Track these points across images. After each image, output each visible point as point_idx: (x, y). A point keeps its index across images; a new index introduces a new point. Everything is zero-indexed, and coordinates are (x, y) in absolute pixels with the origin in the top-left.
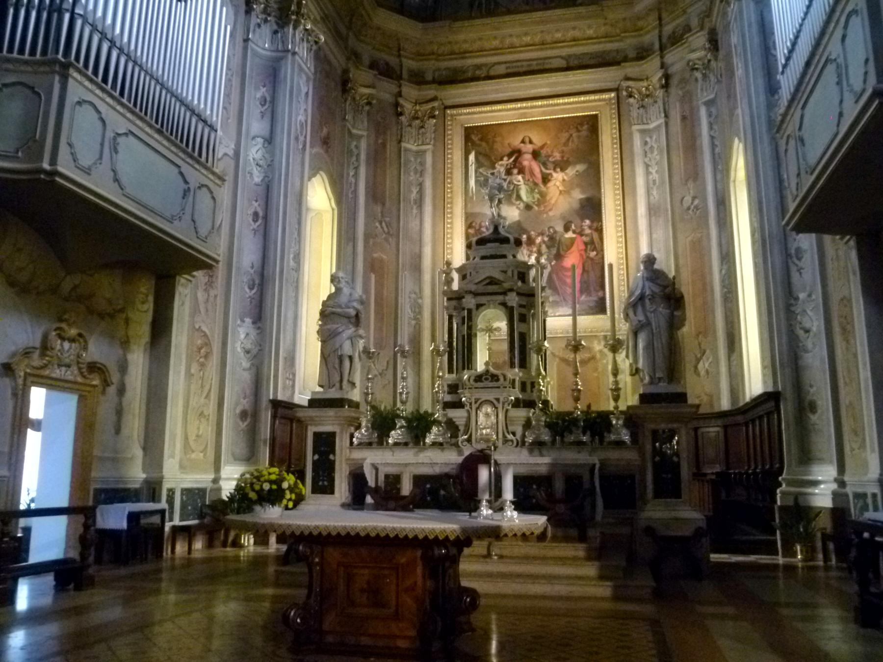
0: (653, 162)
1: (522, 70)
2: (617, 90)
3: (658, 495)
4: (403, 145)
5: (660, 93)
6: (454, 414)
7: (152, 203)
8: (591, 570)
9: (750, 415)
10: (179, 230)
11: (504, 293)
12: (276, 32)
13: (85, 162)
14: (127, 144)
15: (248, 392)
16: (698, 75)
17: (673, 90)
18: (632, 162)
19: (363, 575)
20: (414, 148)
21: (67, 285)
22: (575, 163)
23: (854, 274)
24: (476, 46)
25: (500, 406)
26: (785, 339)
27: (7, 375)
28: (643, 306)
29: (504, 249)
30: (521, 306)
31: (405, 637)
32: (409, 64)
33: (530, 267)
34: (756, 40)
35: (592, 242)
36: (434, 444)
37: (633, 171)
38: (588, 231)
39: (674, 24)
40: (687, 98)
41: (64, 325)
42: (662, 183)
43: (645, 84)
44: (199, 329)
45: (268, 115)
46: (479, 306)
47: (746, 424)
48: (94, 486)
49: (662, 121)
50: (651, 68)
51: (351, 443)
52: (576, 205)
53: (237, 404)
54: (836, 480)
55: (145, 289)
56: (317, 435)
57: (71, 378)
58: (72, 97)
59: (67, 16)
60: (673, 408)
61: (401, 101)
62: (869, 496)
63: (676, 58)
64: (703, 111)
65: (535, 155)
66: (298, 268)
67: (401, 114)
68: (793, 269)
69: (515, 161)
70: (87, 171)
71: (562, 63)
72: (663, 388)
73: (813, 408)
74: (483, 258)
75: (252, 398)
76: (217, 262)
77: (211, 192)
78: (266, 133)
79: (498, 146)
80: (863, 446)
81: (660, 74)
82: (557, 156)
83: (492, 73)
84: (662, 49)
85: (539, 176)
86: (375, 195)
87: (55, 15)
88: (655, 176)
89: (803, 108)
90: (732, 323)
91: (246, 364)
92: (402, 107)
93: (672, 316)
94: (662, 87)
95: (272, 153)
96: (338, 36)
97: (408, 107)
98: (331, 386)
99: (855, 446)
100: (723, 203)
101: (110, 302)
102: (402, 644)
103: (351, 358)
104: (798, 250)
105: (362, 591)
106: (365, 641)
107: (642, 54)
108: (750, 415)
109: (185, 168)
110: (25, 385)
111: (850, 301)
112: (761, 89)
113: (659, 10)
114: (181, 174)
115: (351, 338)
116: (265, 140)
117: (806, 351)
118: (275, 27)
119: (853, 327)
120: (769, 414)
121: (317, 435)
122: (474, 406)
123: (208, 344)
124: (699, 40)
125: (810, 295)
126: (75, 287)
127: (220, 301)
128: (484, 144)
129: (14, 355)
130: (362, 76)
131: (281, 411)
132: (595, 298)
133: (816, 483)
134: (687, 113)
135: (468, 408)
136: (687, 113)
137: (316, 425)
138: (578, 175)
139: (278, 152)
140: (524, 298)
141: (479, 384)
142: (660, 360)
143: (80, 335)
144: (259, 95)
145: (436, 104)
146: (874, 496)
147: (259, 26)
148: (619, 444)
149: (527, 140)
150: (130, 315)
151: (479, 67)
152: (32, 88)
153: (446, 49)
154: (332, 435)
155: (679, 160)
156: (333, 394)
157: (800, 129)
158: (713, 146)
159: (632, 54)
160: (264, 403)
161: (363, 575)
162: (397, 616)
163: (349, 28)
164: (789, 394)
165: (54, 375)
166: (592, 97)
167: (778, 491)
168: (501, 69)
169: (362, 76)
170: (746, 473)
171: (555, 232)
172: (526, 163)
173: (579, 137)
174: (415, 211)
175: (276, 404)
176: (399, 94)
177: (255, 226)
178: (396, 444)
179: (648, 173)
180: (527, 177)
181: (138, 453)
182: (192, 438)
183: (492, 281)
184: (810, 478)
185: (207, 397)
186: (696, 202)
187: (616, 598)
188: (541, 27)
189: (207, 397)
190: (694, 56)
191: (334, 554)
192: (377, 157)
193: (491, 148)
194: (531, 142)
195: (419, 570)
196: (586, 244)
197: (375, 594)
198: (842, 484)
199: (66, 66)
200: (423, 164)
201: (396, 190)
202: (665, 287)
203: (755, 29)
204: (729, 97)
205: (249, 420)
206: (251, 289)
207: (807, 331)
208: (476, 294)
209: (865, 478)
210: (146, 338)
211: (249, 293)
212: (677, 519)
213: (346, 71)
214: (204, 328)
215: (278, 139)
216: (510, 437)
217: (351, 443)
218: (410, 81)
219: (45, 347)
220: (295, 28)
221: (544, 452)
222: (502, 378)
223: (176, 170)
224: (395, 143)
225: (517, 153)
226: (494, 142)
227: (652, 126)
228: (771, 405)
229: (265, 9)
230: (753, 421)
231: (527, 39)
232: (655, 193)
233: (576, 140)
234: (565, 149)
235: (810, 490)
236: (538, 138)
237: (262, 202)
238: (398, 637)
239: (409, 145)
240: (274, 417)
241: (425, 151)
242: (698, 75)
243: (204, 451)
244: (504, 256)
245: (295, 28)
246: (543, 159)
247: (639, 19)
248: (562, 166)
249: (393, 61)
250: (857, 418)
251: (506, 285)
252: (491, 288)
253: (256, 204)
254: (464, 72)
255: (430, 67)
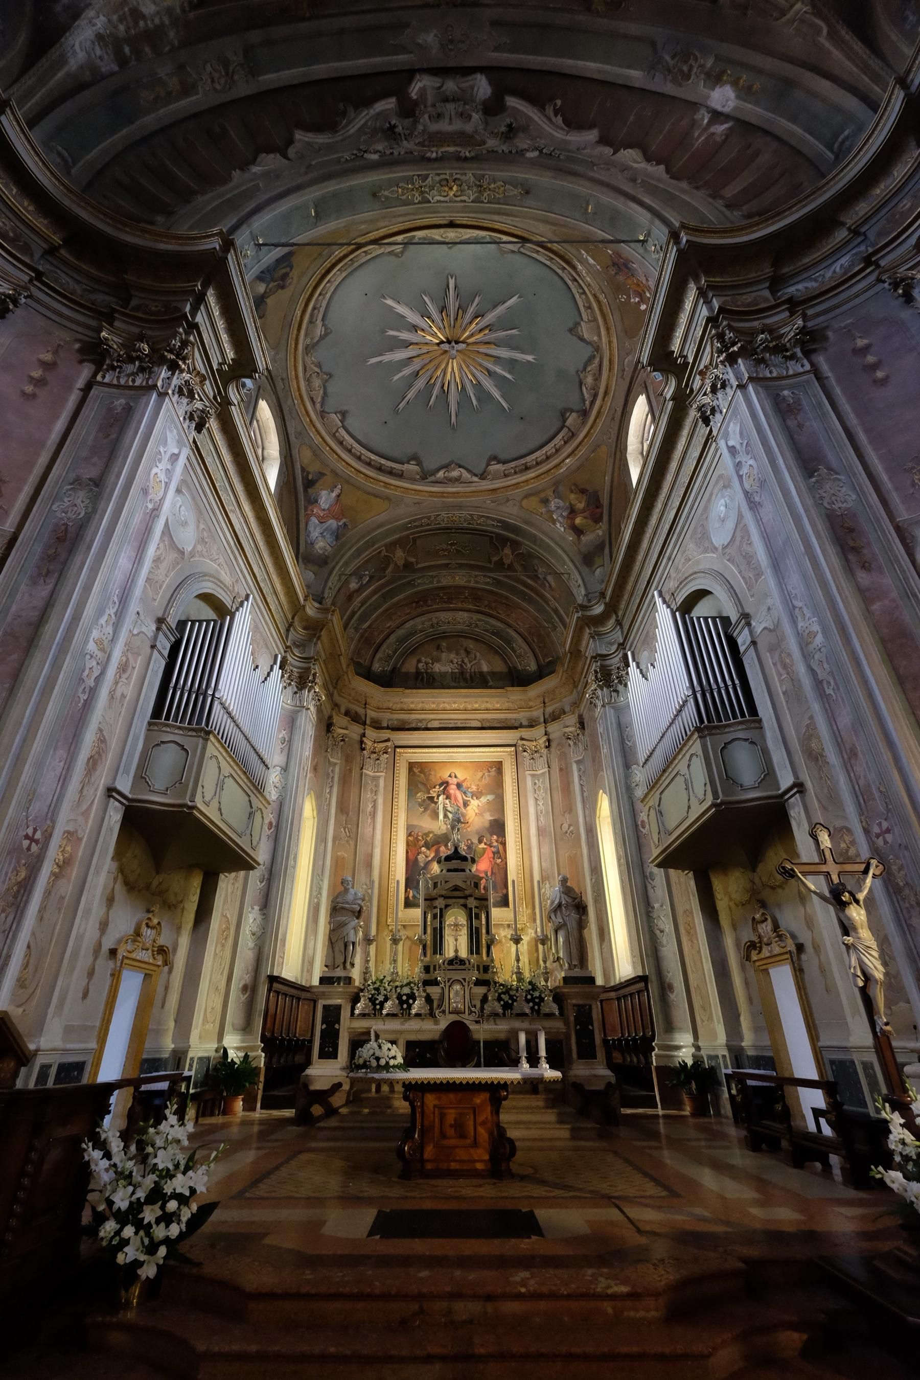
0: (540, 798)
1: (450, 726)
2: (515, 745)
3: (580, 1057)
4: (364, 771)
5: (544, 751)
6: (431, 990)
7: (234, 825)
8: (550, 1116)
9: (622, 992)
10: (244, 843)
11: (466, 897)
12: (296, 693)
13: (207, 799)
14: (229, 782)
15: (250, 968)
16: (571, 743)
17: (553, 749)
18: (526, 797)
19: (451, 1115)
20: (371, 774)
21: (155, 883)
22: (487, 794)
23: (694, 896)
24: (420, 706)
25: (466, 984)
26: (647, 936)
27: (110, 959)
28: (561, 912)
29: (461, 865)
30: (476, 907)
31: (482, 1161)
32: (372, 714)
33: (481, 878)
34: (616, 734)
35: (498, 852)
36: (418, 1015)
37: (527, 802)
38: (495, 844)
39: (554, 707)
40: (563, 756)
41: (150, 915)
42: (547, 812)
43: (534, 744)
44: (226, 916)
45: (286, 751)
46: (447, 906)
47: (618, 999)
48: (144, 1057)
49: (547, 770)
50: (539, 731)
51: (352, 1014)
52: (487, 824)
53: (240, 980)
54: (693, 1045)
55: (196, 882)
56: (325, 1007)
57: (146, 960)
58: (208, 754)
59: (209, 699)
60: (586, 988)
61: (364, 739)
62: (720, 1057)
63: (555, 729)
64: (575, 767)
65: (459, 786)
66: (294, 867)
67: (364, 749)
68: (649, 887)
69: (444, 789)
70: (207, 804)
71: (479, 725)
72: (577, 972)
73: (671, 988)
74: (449, 871)
75: (253, 974)
76: (259, 864)
77: (262, 813)
78: (283, 764)
79: (432, 777)
80: (710, 1018)
81: (545, 738)
82: (474, 788)
83: (429, 726)
84: (545, 722)
85: (461, 801)
86: (342, 808)
87: (201, 698)
88: (541, 807)
89: (661, 793)
90: (602, 919)
91: (251, 944)
92: (365, 744)
93: (580, 919)
94: (546, 747)
95: (286, 779)
96: (330, 695)
97: (369, 743)
98: (335, 967)
99: (704, 1018)
100: (592, 832)
101: (176, 894)
102: (479, 1166)
103: (354, 943)
104: (651, 873)
105: (451, 1126)
106: (454, 1166)
107: (532, 725)
108: (622, 992)
109: (253, 798)
110: (121, 966)
111: (691, 913)
112: (620, 763)
113: (544, 697)
114: (250, 801)
115: (355, 928)
116: (282, 768)
117: (663, 946)
118: (296, 690)
119: (696, 932)
120: (639, 992)
121: (325, 1007)
122: (448, 984)
123: (228, 928)
124: (571, 720)
125: (662, 906)
126: (160, 884)
127: (239, 893)
128: (422, 775)
129: (119, 941)
130: (340, 720)
131: (276, 986)
132: (501, 895)
133: (678, 1048)
134: (563, 767)
135: (442, 985)
136: (563, 767)
137: (326, 999)
138: (489, 802)
139: (290, 777)
140: (478, 902)
141: (451, 967)
142: (574, 951)
143: (159, 923)
144: (280, 736)
145: (389, 744)
146: (724, 1056)
147: (285, 688)
148: (550, 1015)
149: (453, 775)
150: (186, 906)
151: (421, 721)
152: (182, 747)
153: (399, 706)
154: (338, 1008)
155: (558, 797)
156: (339, 973)
157: (659, 805)
158: (582, 791)
159: (525, 723)
160: (263, 978)
161: (451, 1115)
162: (475, 1144)
163: (335, 688)
164: (653, 978)
165: (138, 958)
166: (499, 749)
167: (653, 1054)
168: (436, 724)
169: (340, 720)
170: (619, 1040)
171: (472, 843)
172: (452, 792)
173: (489, 776)
174: (369, 821)
175: (274, 980)
176: (363, 735)
177: (269, 832)
178: (388, 1015)
179: (537, 805)
180: (453, 801)
181: (172, 1024)
182: (209, 1010)
183: (456, 888)
184: (676, 1043)
185: (222, 974)
186: (572, 828)
187: (574, 1138)
188: (466, 700)
189: (222, 974)
190: (567, 730)
191: (430, 1099)
192: (345, 781)
193: (428, 780)
194: (456, 777)
195: (489, 1108)
196: (494, 853)
197: (459, 1128)
198: (698, 1048)
199: (208, 733)
200: (377, 786)
201: (357, 804)
202: (575, 899)
203: (615, 726)
204: (594, 761)
205: (248, 993)
206: (261, 882)
207: (662, 931)
208: (446, 897)
209: (716, 1044)
210: (190, 924)
211: (260, 886)
212: (595, 1076)
213: (330, 717)
214: (228, 916)
215: (291, 769)
216: (473, 1009)
217: (352, 1014)
218: (370, 726)
219: (138, 933)
220: (309, 691)
221: (498, 1022)
222: (467, 962)
223: (247, 798)
224: (358, 769)
225: (445, 784)
226: (430, 774)
227: (539, 772)
228: (642, 985)
229: (289, 677)
230: (625, 997)
231: (455, 706)
232: (542, 819)
233: (487, 778)
234: (480, 783)
235: (676, 1053)
236: (461, 775)
237: (276, 816)
238: (478, 1161)
239: (368, 772)
240: (269, 990)
241: (379, 777)
242: (571, 743)
243: (214, 1022)
244: (463, 870)
245: (309, 691)
246: (464, 789)
247: (530, 700)
248: (477, 795)
249: (361, 711)
250: (705, 997)
251: (467, 892)
252: (457, 893)
253: (271, 816)
254: (409, 723)
255: (386, 718)
